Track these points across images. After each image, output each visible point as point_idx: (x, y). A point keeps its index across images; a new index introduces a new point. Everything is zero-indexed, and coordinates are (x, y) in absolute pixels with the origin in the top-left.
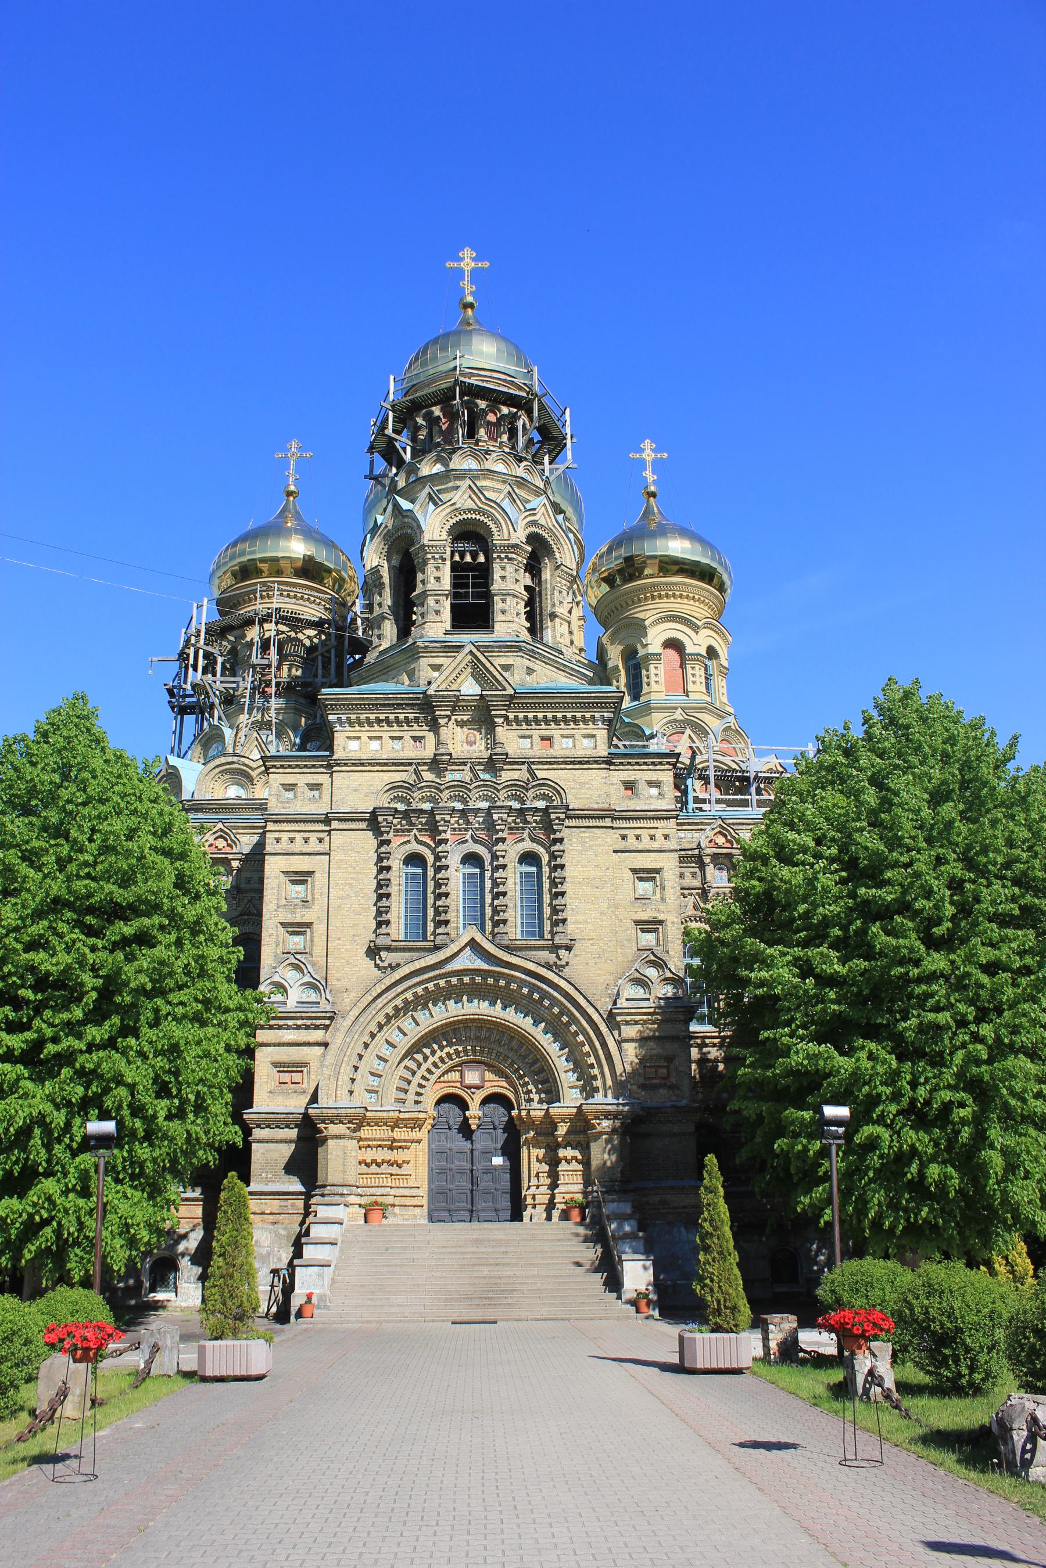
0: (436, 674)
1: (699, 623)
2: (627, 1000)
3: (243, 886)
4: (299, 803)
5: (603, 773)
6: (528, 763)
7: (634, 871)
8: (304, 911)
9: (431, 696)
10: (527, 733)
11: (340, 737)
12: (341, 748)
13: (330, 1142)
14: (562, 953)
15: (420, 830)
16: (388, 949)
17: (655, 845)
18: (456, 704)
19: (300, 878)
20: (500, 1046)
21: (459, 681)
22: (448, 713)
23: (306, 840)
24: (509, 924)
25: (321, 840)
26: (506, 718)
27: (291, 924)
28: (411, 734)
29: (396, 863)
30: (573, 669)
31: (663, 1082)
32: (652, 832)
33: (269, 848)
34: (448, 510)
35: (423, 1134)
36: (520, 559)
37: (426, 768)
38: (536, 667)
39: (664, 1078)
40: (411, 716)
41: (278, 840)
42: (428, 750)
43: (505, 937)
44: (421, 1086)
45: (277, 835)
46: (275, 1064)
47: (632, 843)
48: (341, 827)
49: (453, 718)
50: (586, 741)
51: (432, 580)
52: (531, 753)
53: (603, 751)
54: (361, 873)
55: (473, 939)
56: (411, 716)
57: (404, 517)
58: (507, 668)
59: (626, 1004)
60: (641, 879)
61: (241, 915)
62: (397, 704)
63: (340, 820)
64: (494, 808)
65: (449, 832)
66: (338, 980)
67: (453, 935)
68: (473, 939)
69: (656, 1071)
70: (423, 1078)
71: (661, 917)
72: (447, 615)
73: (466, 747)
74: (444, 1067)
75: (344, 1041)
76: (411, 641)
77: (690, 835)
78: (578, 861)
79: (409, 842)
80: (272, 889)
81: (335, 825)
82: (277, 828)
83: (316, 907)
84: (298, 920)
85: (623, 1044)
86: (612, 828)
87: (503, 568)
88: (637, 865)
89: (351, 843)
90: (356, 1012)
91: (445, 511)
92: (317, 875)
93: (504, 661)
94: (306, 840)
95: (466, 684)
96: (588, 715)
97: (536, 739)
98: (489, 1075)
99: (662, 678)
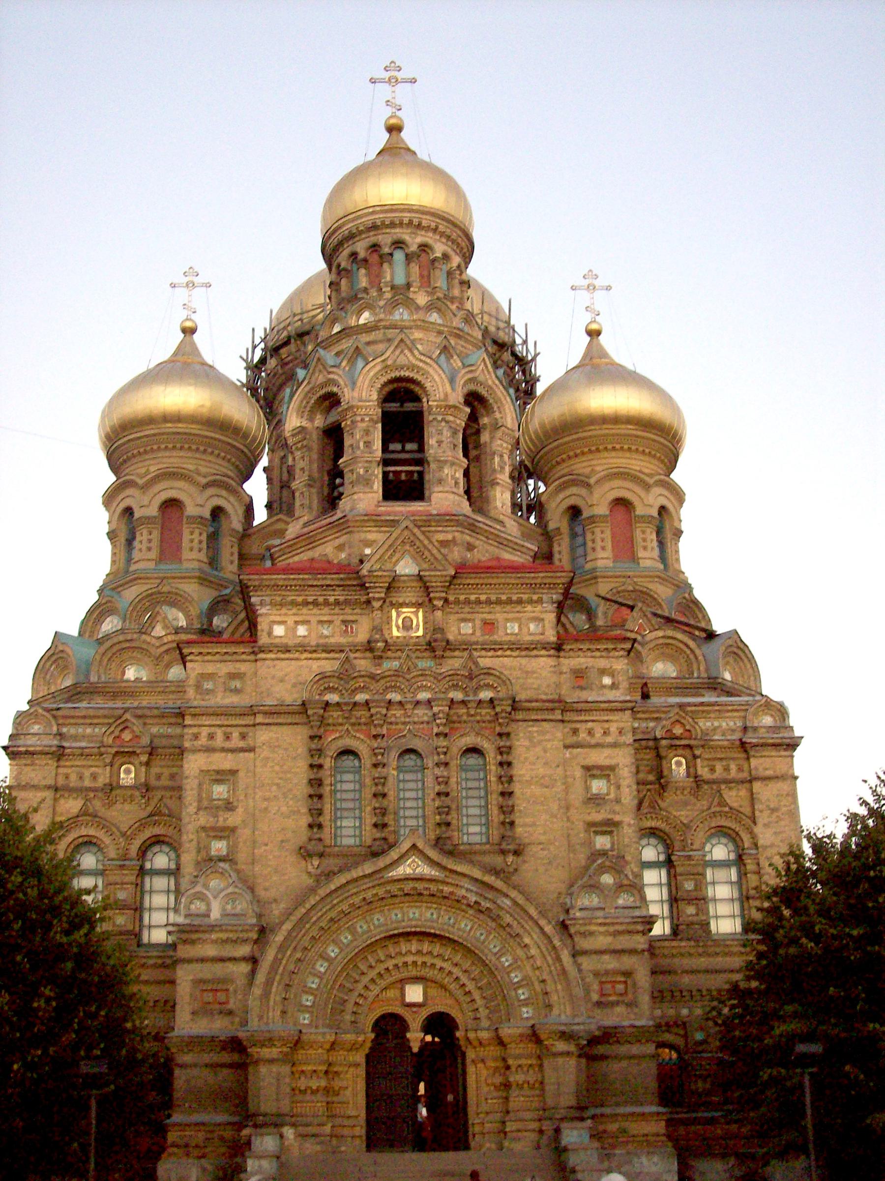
0: (368, 551)
2: (581, 909)
3: (153, 782)
4: (220, 695)
5: (552, 662)
7: (587, 768)
8: (228, 815)
9: (365, 576)
10: (469, 616)
12: (265, 634)
13: (263, 1070)
14: (510, 858)
15: (353, 725)
16: (321, 855)
17: (609, 739)
20: (445, 960)
21: (394, 560)
22: (383, 595)
23: (228, 738)
24: (452, 827)
25: (243, 737)
26: (446, 600)
27: (213, 829)
28: (341, 618)
29: (328, 763)
30: (516, 544)
31: (620, 998)
32: (606, 725)
34: (378, 368)
35: (360, 1057)
36: (458, 422)
37: (357, 655)
38: (477, 543)
39: (621, 995)
40: (342, 598)
41: (196, 737)
42: (362, 634)
43: (449, 842)
44: (356, 1003)
45: (195, 730)
47: (583, 735)
48: (267, 721)
49: (388, 600)
50: (532, 627)
51: (361, 444)
52: (474, 639)
54: (289, 772)
55: (414, 846)
56: (342, 598)
57: (329, 373)
58: (444, 543)
60: (594, 776)
61: (149, 816)
62: (328, 586)
63: (265, 713)
64: (434, 700)
65: (385, 727)
66: (266, 889)
67: (391, 839)
68: (414, 846)
69: (613, 987)
70: (361, 995)
71: (617, 818)
72: (378, 486)
74: (383, 983)
75: (276, 959)
76: (339, 514)
77: (644, 725)
78: (526, 759)
79: (341, 737)
80: (192, 789)
82: (196, 723)
83: (240, 810)
84: (221, 823)
86: (563, 721)
87: (440, 433)
88: (589, 762)
89: (277, 739)
90: (287, 926)
91: (375, 367)
92: (241, 774)
93: (441, 537)
94: (228, 738)
95: (402, 563)
96: (535, 597)
97: (478, 623)
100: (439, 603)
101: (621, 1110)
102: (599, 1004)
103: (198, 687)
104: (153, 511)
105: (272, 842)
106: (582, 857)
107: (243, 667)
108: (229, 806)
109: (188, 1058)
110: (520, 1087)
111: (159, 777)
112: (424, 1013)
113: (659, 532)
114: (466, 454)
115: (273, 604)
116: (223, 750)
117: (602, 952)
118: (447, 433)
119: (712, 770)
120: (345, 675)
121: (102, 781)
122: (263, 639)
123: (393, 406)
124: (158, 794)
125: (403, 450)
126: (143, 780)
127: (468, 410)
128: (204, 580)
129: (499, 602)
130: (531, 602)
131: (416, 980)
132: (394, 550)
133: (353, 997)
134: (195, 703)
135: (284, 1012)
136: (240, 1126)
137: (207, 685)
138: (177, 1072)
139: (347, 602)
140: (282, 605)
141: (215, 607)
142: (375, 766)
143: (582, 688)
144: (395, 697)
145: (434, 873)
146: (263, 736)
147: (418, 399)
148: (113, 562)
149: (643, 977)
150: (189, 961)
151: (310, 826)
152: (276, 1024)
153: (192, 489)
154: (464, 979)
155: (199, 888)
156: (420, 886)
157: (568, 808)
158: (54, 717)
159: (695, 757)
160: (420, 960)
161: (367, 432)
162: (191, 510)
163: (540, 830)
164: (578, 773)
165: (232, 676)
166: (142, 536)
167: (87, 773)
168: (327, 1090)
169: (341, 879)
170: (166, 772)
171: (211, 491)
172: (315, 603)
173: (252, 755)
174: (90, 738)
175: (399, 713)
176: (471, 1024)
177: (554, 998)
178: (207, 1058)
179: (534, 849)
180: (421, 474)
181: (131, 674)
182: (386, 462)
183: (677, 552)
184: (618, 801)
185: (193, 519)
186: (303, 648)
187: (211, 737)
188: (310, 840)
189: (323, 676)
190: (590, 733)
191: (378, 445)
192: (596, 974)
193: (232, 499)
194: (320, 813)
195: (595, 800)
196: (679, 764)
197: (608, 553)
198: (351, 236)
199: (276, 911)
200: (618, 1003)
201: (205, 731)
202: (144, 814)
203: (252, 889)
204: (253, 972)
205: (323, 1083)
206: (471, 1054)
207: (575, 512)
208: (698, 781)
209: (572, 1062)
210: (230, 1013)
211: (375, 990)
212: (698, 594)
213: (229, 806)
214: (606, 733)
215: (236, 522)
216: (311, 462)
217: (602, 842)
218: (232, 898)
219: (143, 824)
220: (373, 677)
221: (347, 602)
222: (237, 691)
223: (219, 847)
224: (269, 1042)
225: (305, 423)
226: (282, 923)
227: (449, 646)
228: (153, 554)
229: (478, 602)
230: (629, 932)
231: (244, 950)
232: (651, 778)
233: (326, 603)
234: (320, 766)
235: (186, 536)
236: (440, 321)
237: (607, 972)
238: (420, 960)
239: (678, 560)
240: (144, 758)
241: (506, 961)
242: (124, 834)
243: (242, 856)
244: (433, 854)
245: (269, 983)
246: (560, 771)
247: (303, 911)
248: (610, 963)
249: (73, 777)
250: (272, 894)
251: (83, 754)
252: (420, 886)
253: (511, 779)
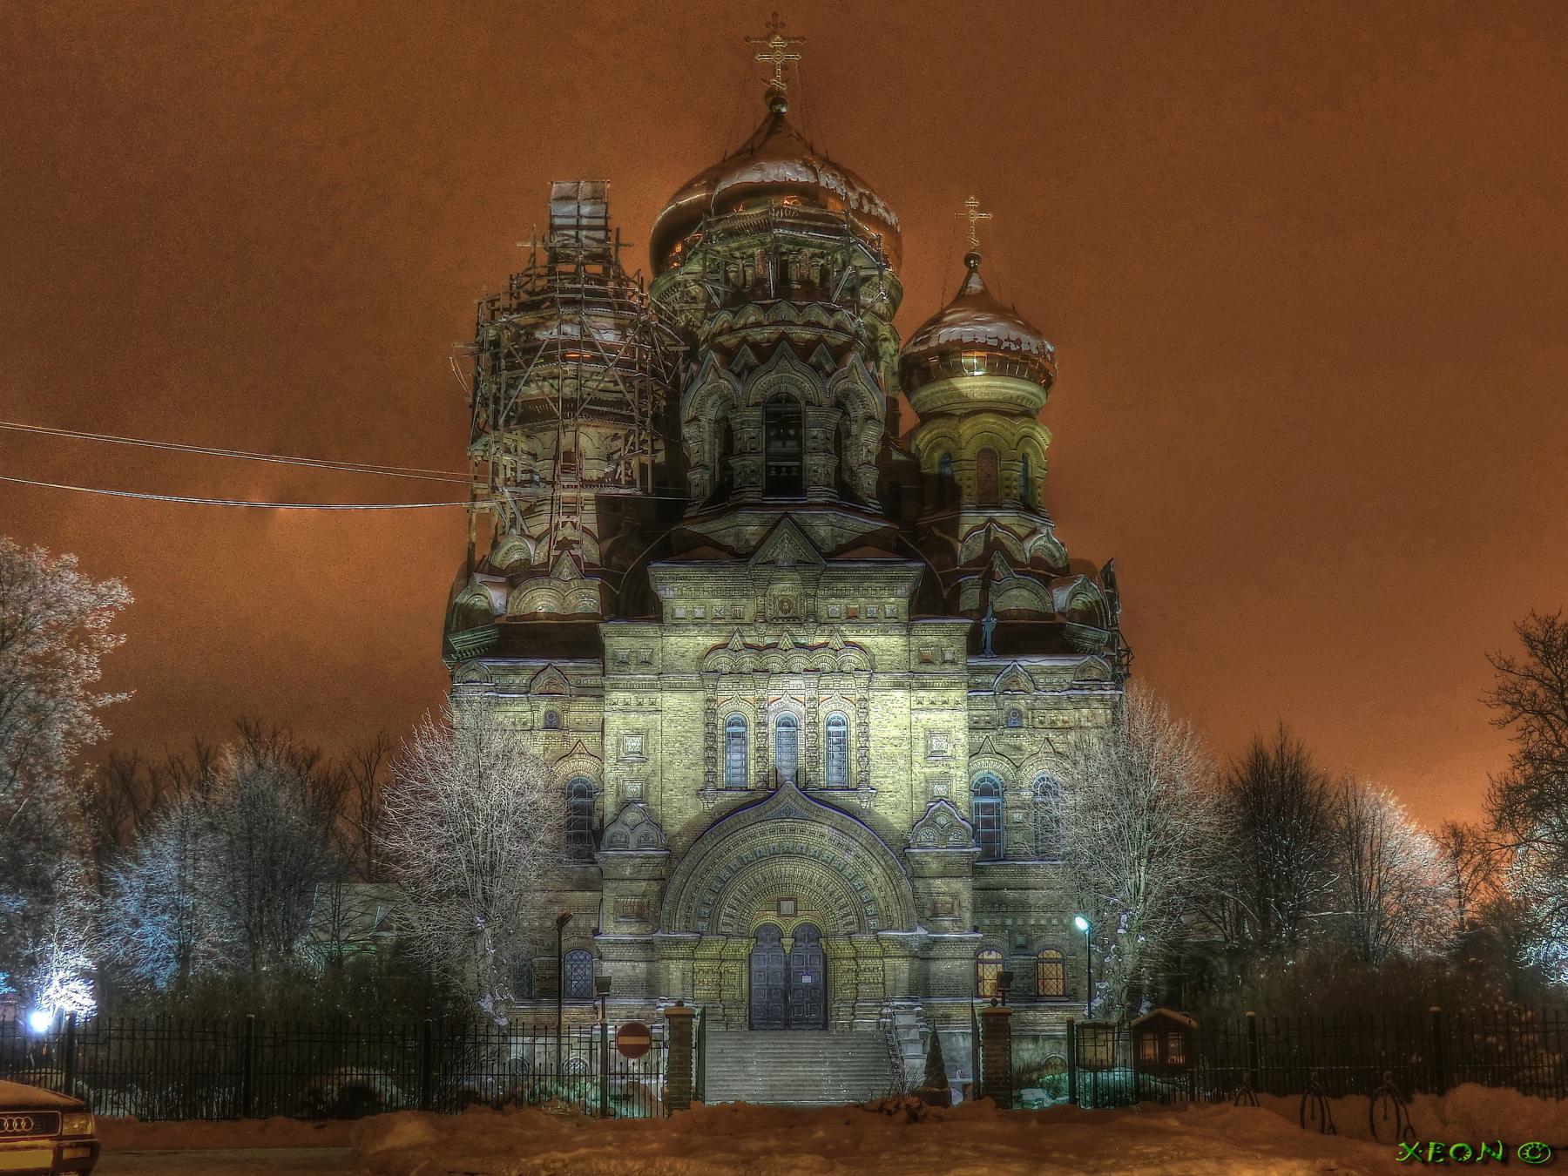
54: (690, 732)
105: (676, 788)
112: (796, 922)
163: (890, 781)
180: (800, 469)
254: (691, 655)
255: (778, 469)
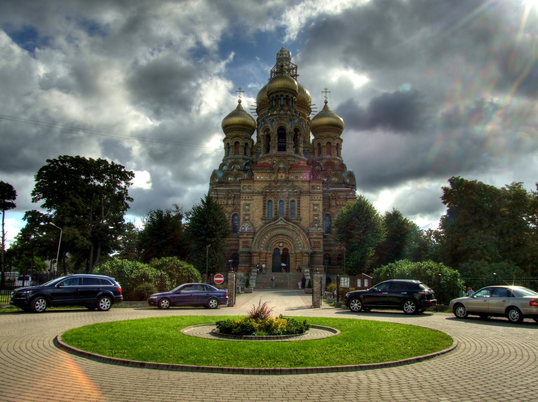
0: (274, 162)
1: (335, 138)
3: (235, 203)
5: (308, 184)
6: (293, 181)
11: (255, 176)
13: (254, 257)
14: (299, 221)
16: (265, 220)
17: (318, 199)
18: (279, 169)
19: (248, 205)
23: (248, 197)
25: (251, 197)
26: (289, 172)
29: (267, 203)
33: (241, 199)
35: (271, 255)
41: (243, 197)
42: (273, 178)
46: (243, 242)
50: (305, 177)
53: (308, 179)
58: (289, 161)
59: (311, 231)
60: (315, 206)
67: (278, 217)
71: (319, 214)
72: (277, 148)
73: (281, 178)
76: (269, 154)
81: (254, 194)
83: (251, 211)
85: (311, 239)
87: (289, 138)
90: (259, 233)
93: (288, 159)
94: (248, 197)
97: (295, 177)
98: (284, 244)
99: (326, 152)
100: (287, 173)
101: (317, 266)
102: (314, 247)
103: (243, 188)
104: (233, 144)
106: (312, 221)
107: (251, 184)
108: (249, 210)
109: (241, 255)
110: (299, 261)
111: (236, 202)
112: (283, 248)
113: (337, 148)
114: (294, 140)
115: (256, 172)
116: (247, 200)
117: (315, 238)
118: (290, 138)
119: (340, 203)
120: (270, 186)
121: (225, 203)
122: (255, 179)
123: (280, 132)
124: (235, 206)
125: (282, 140)
126: (233, 203)
127: (294, 133)
128: (243, 159)
129: (298, 172)
130: (304, 172)
131: (281, 242)
132: (279, 162)
133: (270, 245)
134: (242, 191)
135: (258, 248)
136: (250, 267)
137: (245, 188)
138: (240, 257)
139: (270, 172)
140: (258, 173)
141: (247, 164)
142: (275, 203)
143: (313, 189)
144: (279, 190)
145: (285, 224)
146: (255, 197)
147: (285, 130)
148: (225, 154)
149: (322, 243)
150: (242, 238)
151: (263, 214)
152: (257, 250)
153: (241, 139)
154: (290, 242)
155: (243, 225)
156: (282, 226)
157: (310, 212)
158: (216, 191)
159: (337, 200)
160: (282, 239)
161: (275, 138)
162: (241, 144)
164: (312, 205)
165: (249, 186)
166: (231, 149)
167: (222, 201)
168: (265, 261)
169: (268, 225)
170: (237, 201)
171: (245, 139)
172: (264, 172)
173: (253, 201)
174: (223, 195)
175: (279, 194)
176: (291, 250)
177: (305, 246)
178: (244, 255)
179: (303, 219)
180: (285, 145)
181: (229, 179)
182: (278, 143)
183: (341, 153)
184: (319, 210)
185: (241, 146)
186: (262, 181)
187: (245, 197)
188: (263, 217)
189: (266, 187)
190: (315, 198)
191: (277, 140)
192: (313, 242)
193: (249, 141)
194: (265, 212)
195: (315, 210)
196: (334, 201)
197: (326, 154)
198: (272, 93)
199: (257, 229)
200: (317, 247)
201: (244, 196)
202: (233, 209)
203: (253, 225)
204: (253, 241)
205: (265, 260)
206: (291, 255)
207: (319, 144)
208: (337, 205)
209: (307, 258)
210: (249, 247)
211: (274, 244)
212: (344, 162)
213: (249, 210)
214: (317, 198)
215: (250, 146)
216: (264, 142)
217: (316, 218)
218: (249, 227)
219: (233, 211)
220: (275, 187)
221: (270, 172)
222: (250, 189)
223: (247, 217)
224: (256, 253)
225: (263, 134)
226: (258, 232)
227: (289, 181)
228: (233, 153)
229: (295, 172)
230: (320, 235)
231: (251, 236)
232: (328, 204)
233: (266, 172)
234: (265, 203)
235: (240, 149)
236: (290, 113)
237: (315, 242)
238: (282, 239)
239: (341, 155)
240: (233, 199)
241: (297, 240)
242: (229, 213)
243: (251, 219)
244: (284, 220)
245: (255, 243)
246: (309, 205)
247: (261, 230)
248: (316, 240)
249: (220, 202)
250: (256, 226)
251: (221, 198)
252: (282, 226)
253: (299, 206)
254: (260, 187)
255: (281, 145)
